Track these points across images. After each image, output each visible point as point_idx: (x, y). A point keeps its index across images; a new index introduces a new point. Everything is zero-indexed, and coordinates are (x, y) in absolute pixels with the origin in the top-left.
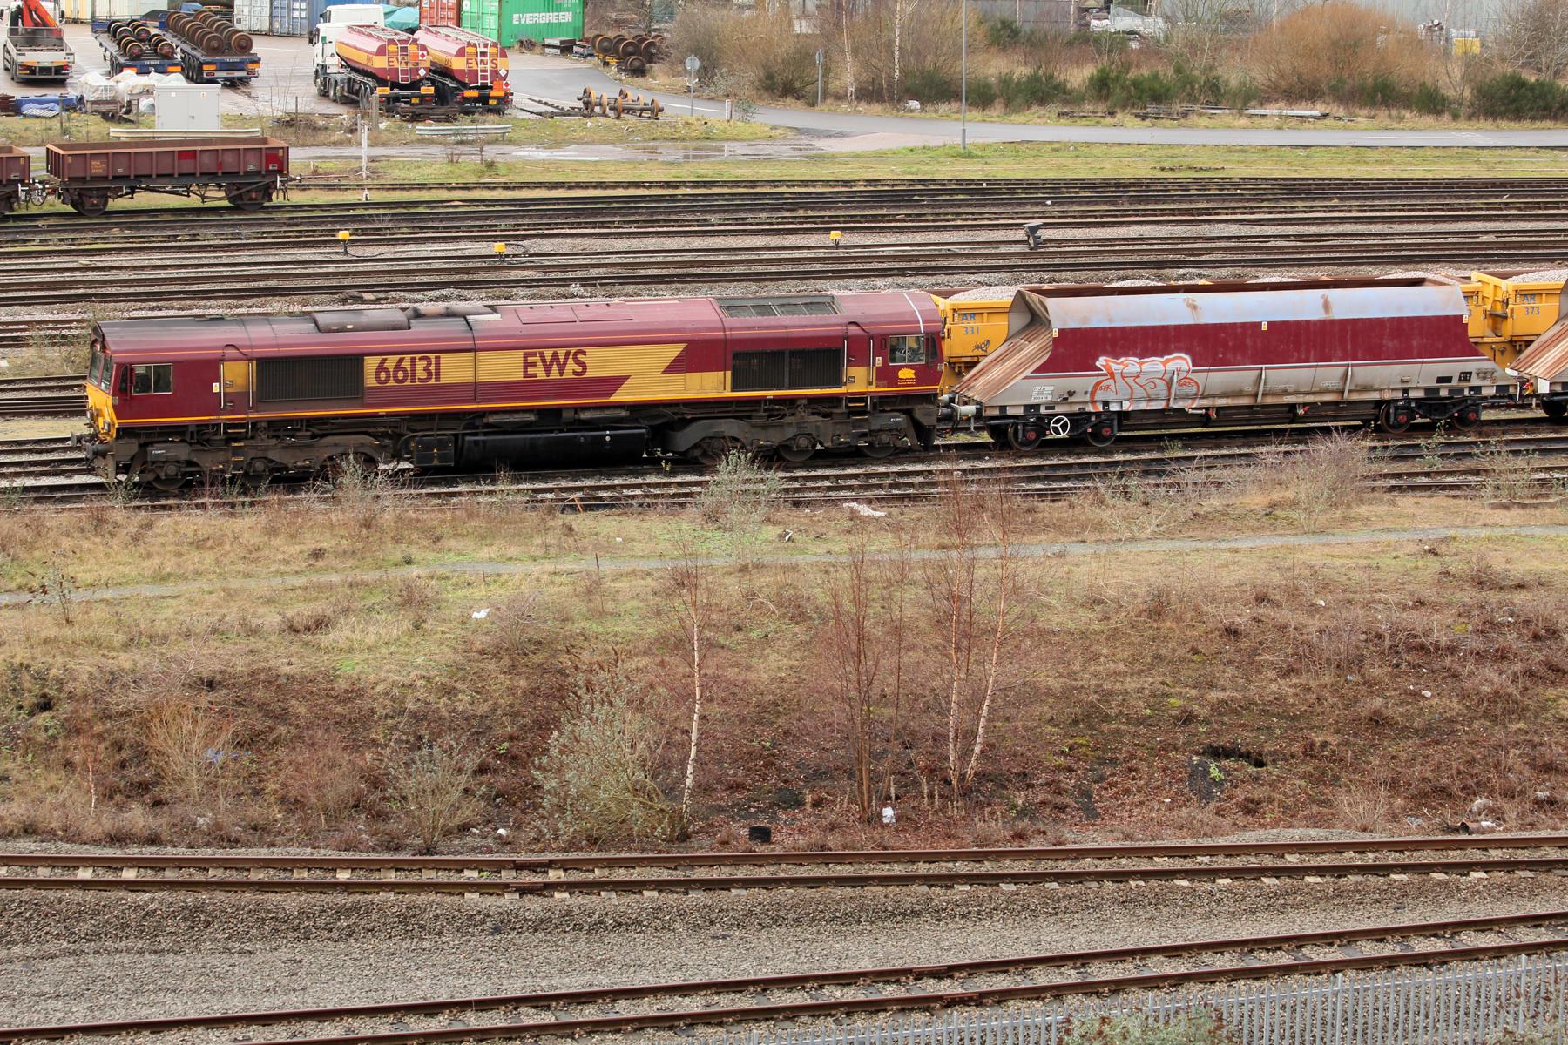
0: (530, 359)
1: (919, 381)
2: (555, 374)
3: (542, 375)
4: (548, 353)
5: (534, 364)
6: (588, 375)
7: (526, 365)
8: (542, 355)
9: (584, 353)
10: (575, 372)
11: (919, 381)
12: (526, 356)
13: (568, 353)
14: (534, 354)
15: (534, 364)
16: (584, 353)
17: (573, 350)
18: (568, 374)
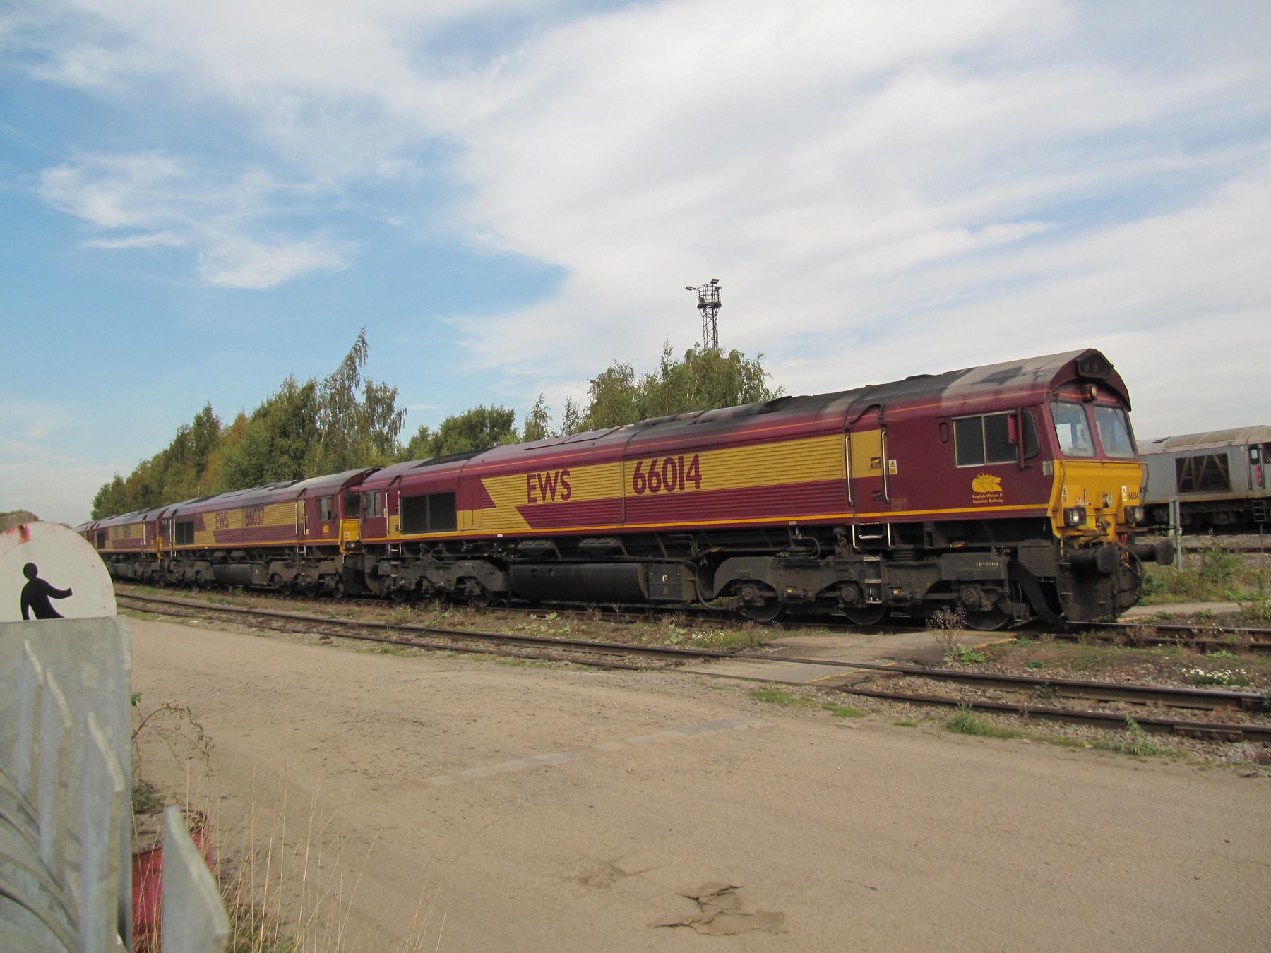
0: (534, 482)
1: (1008, 498)
2: (549, 500)
3: (540, 502)
4: (543, 474)
5: (534, 488)
6: (571, 500)
7: (531, 488)
8: (539, 475)
9: (567, 473)
10: (563, 497)
11: (1008, 498)
12: (530, 478)
13: (557, 473)
14: (533, 477)
15: (534, 488)
16: (567, 473)
17: (560, 471)
18: (558, 500)
